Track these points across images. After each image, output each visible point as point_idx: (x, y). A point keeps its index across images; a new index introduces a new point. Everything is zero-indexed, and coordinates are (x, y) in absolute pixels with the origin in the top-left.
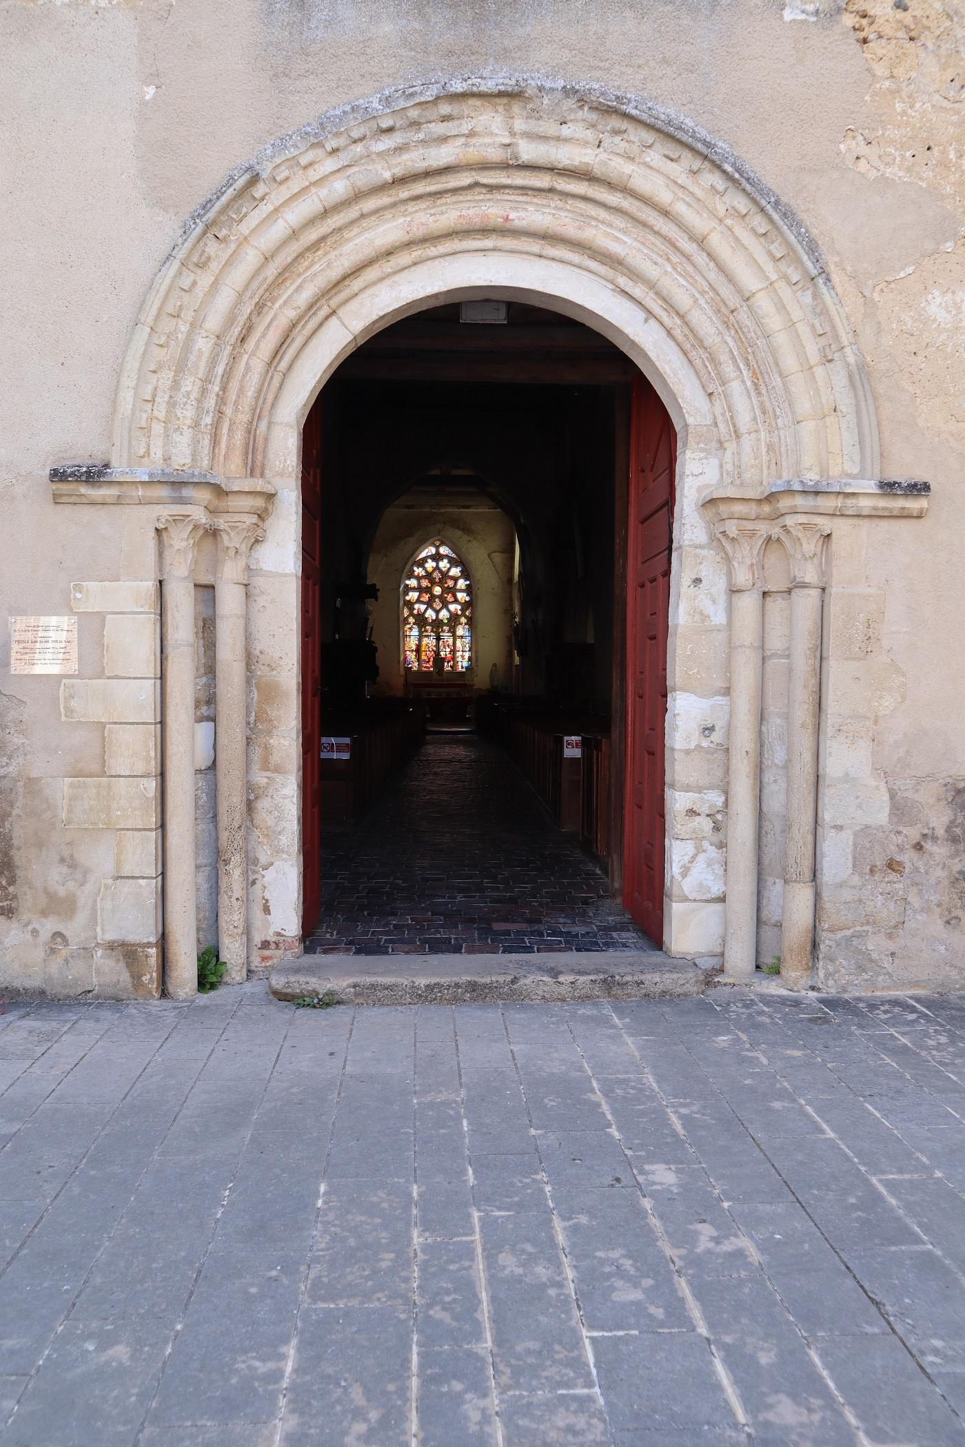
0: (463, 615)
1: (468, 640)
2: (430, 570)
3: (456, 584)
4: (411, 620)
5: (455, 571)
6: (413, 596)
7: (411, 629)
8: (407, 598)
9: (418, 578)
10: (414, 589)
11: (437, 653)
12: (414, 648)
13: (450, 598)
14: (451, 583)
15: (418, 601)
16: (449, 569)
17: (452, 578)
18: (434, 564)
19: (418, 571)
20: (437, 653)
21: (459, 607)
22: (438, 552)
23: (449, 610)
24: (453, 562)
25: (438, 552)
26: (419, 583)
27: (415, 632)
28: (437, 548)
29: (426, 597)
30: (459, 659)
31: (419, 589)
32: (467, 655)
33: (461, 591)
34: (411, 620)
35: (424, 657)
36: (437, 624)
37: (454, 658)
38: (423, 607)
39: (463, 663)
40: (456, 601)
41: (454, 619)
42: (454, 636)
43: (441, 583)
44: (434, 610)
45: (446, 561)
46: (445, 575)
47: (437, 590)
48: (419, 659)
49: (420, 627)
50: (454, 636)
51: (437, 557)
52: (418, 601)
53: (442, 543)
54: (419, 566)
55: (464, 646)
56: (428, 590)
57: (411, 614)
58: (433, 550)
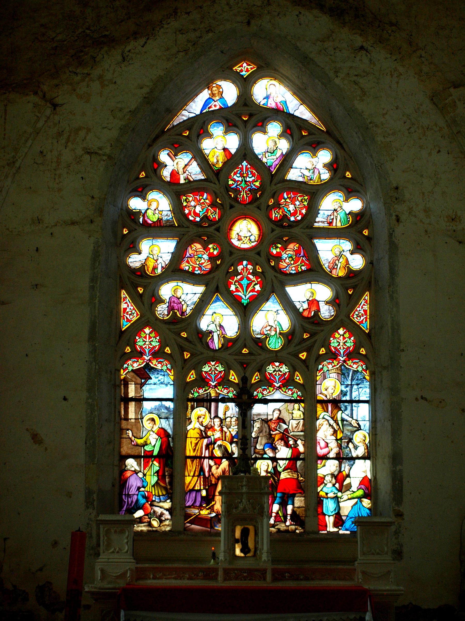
0: (342, 319)
1: (363, 412)
2: (216, 157)
3: (313, 209)
4: (148, 340)
5: (312, 165)
6: (156, 252)
7: (144, 375)
8: (134, 261)
9: (176, 190)
10: (158, 229)
11: (243, 464)
12: (154, 443)
13: (288, 258)
14: (293, 207)
15: (174, 271)
16: (287, 161)
17: (298, 187)
18: (233, 142)
19: (177, 164)
20: (243, 464)
21: (323, 293)
22: (245, 98)
23: (288, 305)
24: (301, 137)
25: (245, 98)
26: (178, 208)
27: (160, 388)
28: (245, 85)
29: (200, 257)
30: (328, 489)
31: (182, 230)
32: (361, 470)
33: (330, 233)
34: (148, 340)
35: (191, 480)
36: (247, 353)
37: (307, 484)
38: (190, 293)
39: (346, 494)
40: (314, 271)
41: (308, 333)
42: (310, 400)
43: (256, 206)
44: (234, 302)
45: (274, 128)
46: (274, 180)
47: (245, 232)
48: (170, 482)
49: (180, 369)
50: (310, 400)
51: (246, 117)
52: (174, 271)
53: (265, 69)
54: (177, 149)
55: (344, 441)
56: (214, 231)
57: (147, 319)
58: (230, 92)
